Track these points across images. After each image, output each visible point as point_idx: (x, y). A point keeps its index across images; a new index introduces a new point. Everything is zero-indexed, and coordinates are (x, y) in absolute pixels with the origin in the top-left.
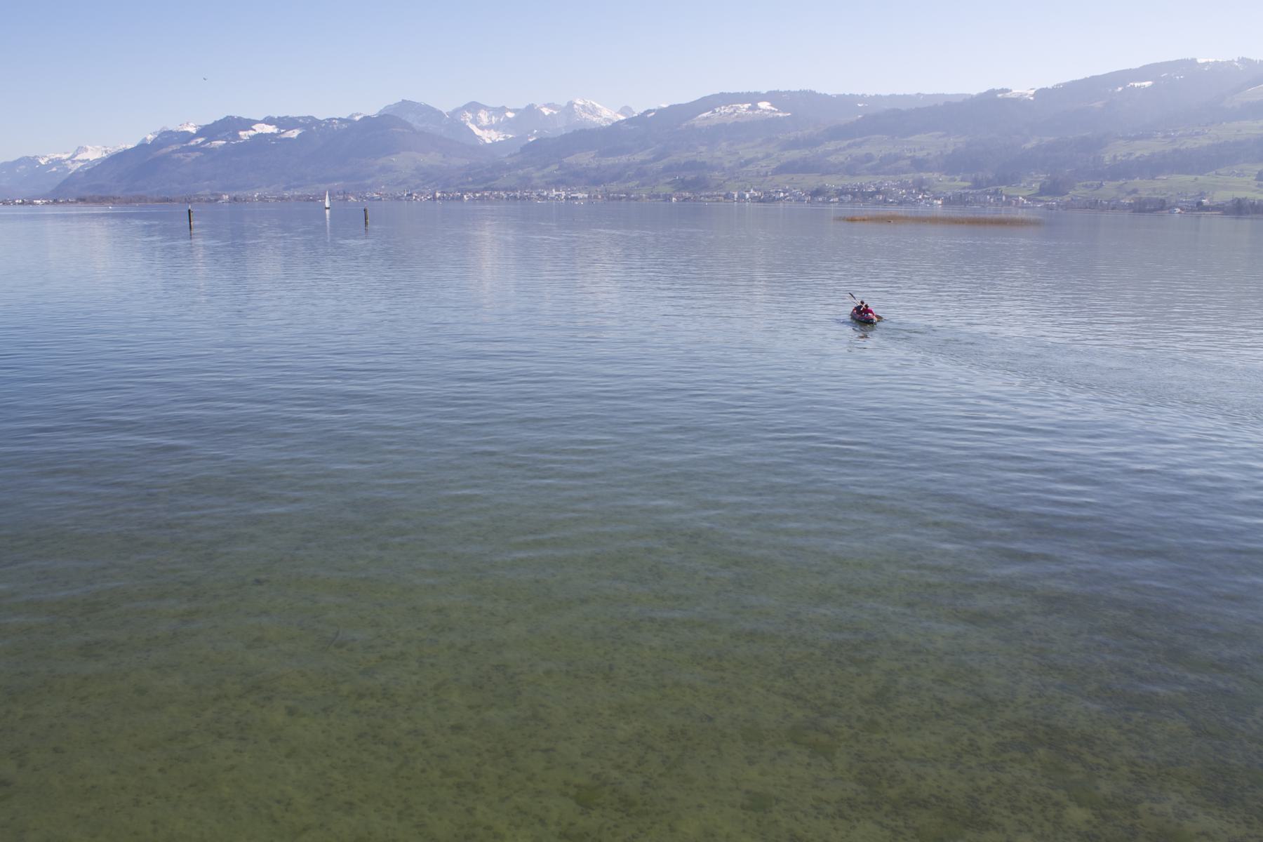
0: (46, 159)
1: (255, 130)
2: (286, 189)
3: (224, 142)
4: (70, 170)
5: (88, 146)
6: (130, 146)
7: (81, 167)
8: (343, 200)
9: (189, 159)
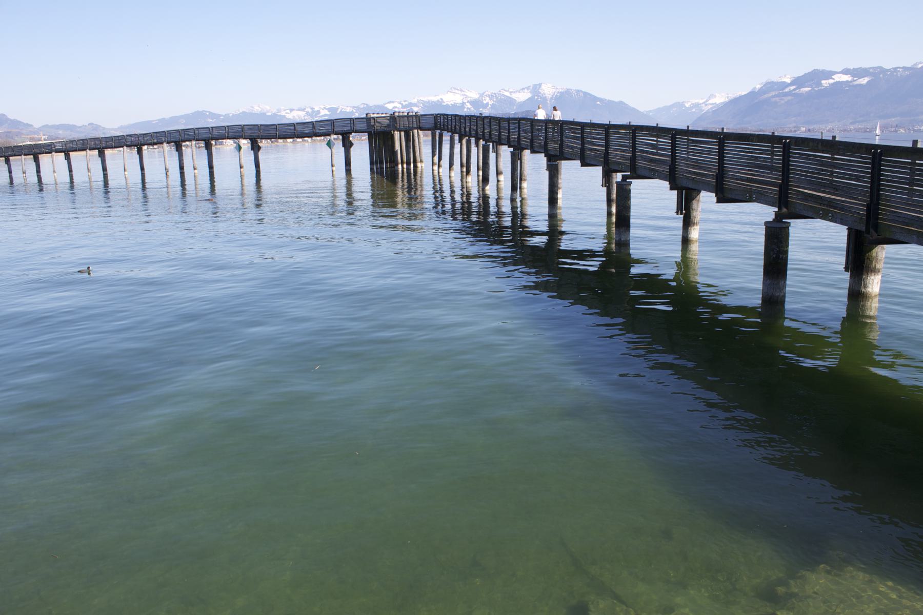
0: (690, 104)
1: (834, 79)
2: (851, 123)
3: (810, 89)
4: (704, 110)
5: (716, 94)
6: (744, 93)
7: (711, 108)
8: (894, 131)
9: (783, 102)
